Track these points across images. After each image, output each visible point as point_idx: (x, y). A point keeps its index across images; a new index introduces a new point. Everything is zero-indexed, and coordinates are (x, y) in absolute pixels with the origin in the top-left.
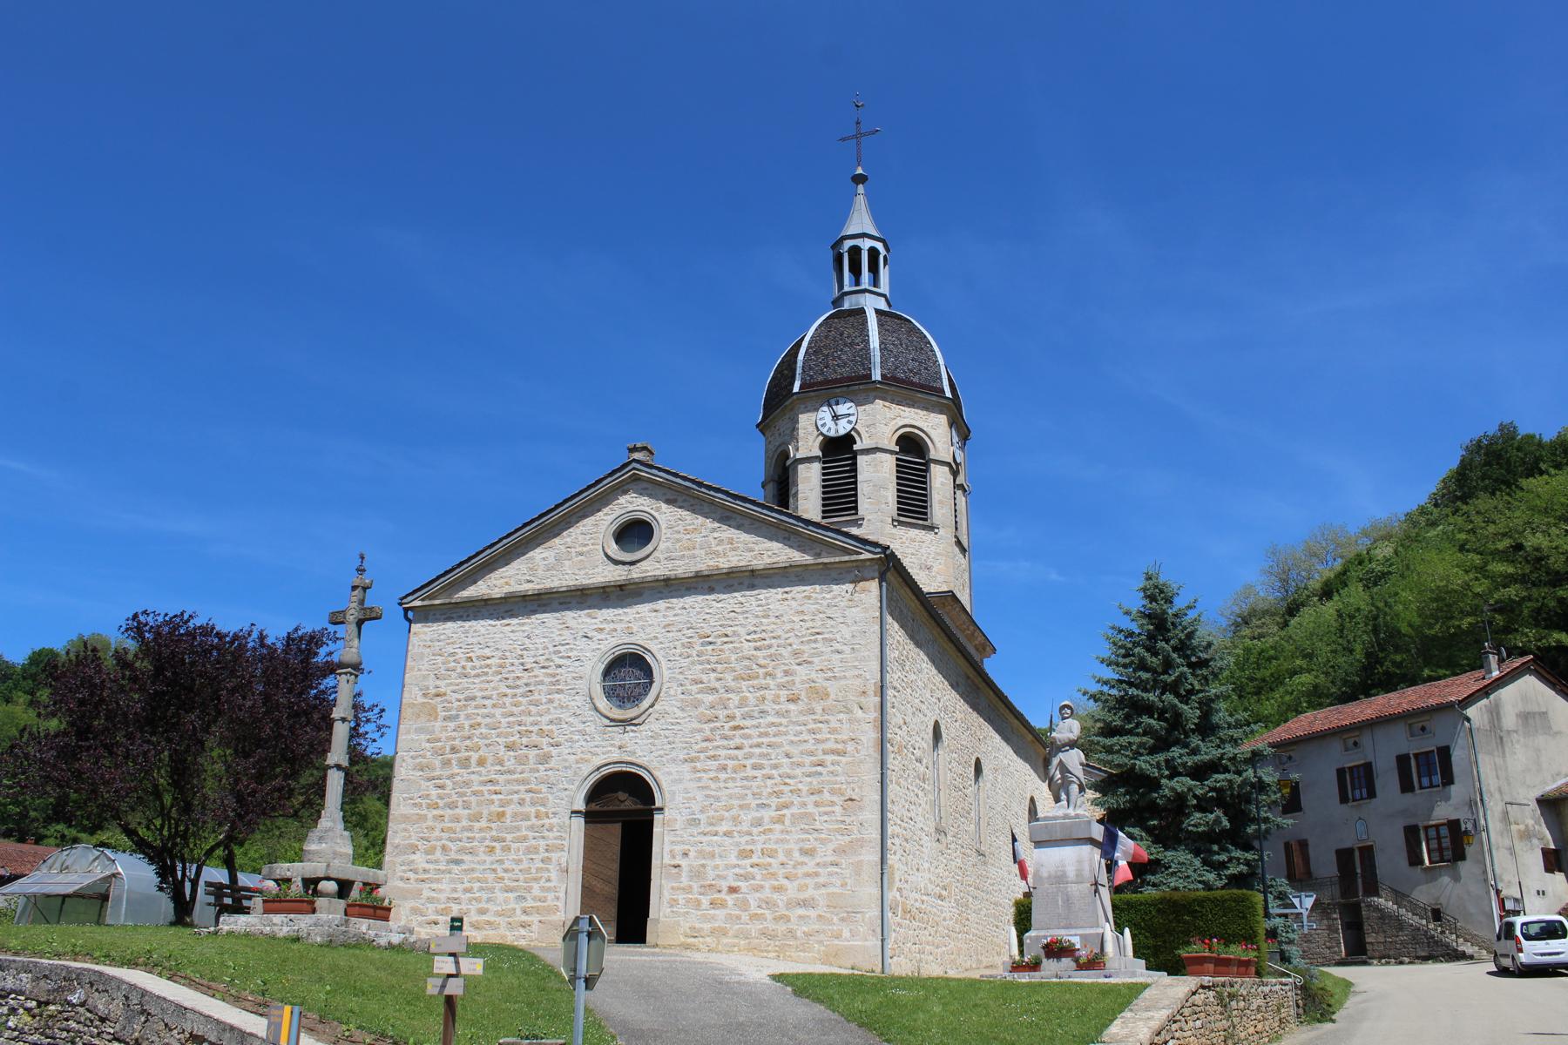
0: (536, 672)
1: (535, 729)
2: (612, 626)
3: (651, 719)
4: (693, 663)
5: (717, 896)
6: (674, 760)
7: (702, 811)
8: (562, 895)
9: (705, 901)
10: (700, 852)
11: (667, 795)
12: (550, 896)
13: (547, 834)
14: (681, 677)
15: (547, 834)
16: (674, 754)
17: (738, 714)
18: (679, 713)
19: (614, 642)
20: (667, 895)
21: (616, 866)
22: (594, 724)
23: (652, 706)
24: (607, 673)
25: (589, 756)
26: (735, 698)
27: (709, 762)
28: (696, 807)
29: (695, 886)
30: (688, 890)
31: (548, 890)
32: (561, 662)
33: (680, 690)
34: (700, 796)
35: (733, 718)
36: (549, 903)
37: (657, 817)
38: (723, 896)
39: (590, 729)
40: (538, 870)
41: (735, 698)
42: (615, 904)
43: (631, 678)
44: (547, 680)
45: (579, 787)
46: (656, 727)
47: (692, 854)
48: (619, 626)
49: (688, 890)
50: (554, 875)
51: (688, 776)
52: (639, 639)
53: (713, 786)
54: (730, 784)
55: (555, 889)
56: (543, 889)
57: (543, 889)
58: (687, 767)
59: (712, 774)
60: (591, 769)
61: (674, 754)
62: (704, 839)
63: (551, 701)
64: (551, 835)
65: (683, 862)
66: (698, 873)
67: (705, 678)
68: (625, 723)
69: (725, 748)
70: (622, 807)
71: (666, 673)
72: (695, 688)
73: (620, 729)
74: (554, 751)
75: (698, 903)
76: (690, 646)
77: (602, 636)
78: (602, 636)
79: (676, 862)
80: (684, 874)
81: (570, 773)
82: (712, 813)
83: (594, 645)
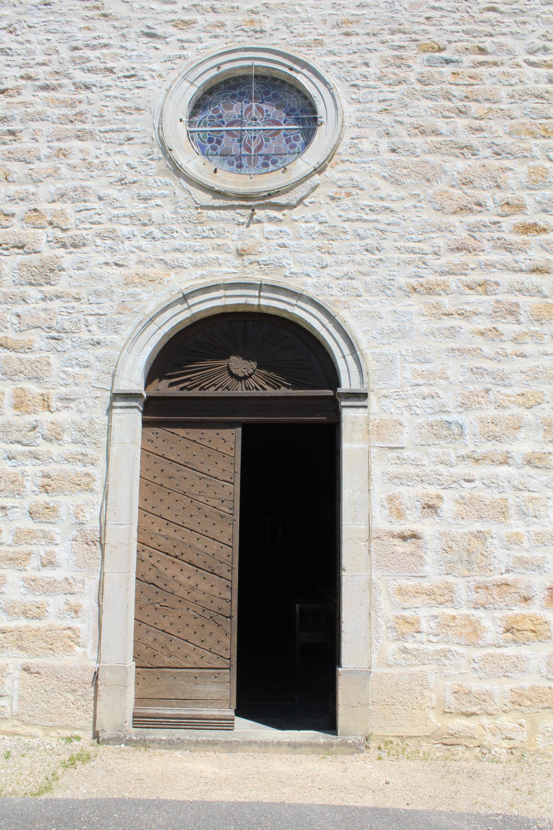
0: (27, 95)
1: (20, 209)
2: (212, 18)
3: (320, 195)
4: (412, 94)
5: (519, 610)
6: (384, 288)
7: (465, 406)
8: (88, 602)
9: (490, 623)
10: (462, 501)
11: (370, 364)
12: (55, 603)
13: (44, 447)
14: (387, 119)
15: (44, 447)
16: (382, 273)
17: (529, 201)
18: (387, 189)
19: (219, 46)
20: (387, 610)
21: (229, 532)
22: (170, 202)
23: (319, 170)
24: (199, 105)
25: (158, 270)
26: (521, 170)
27: (473, 298)
28: (449, 398)
29: (462, 587)
30: (444, 595)
31: (50, 587)
32: (89, 78)
33: (384, 144)
34: (454, 369)
35: (520, 208)
36: (52, 620)
37: (350, 416)
38: (535, 609)
39: (163, 212)
40: (20, 536)
41: (521, 170)
42: (231, 627)
43: (258, 117)
44: (54, 112)
45: (134, 338)
46: (331, 213)
47: (448, 507)
48: (228, 19)
49: (444, 595)
50: (63, 551)
51: (422, 325)
52: (280, 40)
53: (488, 349)
54: (529, 348)
55: (68, 587)
56: (32, 584)
57: (32, 584)
58: (416, 304)
59: (483, 324)
60: (164, 296)
61: (382, 273)
62: (477, 471)
63: (63, 153)
64: (54, 449)
65: (427, 527)
66: (467, 554)
67: (441, 124)
68: (249, 201)
69: (506, 267)
70: (239, 390)
71: (349, 110)
72: (419, 141)
73: (242, 216)
74: (67, 259)
75: (474, 631)
76: (400, 62)
77: (191, 35)
78: (183, 36)
79: (406, 527)
80: (430, 557)
81: (107, 306)
82: (490, 412)
83: (172, 51)
